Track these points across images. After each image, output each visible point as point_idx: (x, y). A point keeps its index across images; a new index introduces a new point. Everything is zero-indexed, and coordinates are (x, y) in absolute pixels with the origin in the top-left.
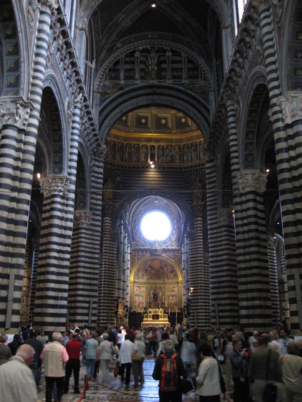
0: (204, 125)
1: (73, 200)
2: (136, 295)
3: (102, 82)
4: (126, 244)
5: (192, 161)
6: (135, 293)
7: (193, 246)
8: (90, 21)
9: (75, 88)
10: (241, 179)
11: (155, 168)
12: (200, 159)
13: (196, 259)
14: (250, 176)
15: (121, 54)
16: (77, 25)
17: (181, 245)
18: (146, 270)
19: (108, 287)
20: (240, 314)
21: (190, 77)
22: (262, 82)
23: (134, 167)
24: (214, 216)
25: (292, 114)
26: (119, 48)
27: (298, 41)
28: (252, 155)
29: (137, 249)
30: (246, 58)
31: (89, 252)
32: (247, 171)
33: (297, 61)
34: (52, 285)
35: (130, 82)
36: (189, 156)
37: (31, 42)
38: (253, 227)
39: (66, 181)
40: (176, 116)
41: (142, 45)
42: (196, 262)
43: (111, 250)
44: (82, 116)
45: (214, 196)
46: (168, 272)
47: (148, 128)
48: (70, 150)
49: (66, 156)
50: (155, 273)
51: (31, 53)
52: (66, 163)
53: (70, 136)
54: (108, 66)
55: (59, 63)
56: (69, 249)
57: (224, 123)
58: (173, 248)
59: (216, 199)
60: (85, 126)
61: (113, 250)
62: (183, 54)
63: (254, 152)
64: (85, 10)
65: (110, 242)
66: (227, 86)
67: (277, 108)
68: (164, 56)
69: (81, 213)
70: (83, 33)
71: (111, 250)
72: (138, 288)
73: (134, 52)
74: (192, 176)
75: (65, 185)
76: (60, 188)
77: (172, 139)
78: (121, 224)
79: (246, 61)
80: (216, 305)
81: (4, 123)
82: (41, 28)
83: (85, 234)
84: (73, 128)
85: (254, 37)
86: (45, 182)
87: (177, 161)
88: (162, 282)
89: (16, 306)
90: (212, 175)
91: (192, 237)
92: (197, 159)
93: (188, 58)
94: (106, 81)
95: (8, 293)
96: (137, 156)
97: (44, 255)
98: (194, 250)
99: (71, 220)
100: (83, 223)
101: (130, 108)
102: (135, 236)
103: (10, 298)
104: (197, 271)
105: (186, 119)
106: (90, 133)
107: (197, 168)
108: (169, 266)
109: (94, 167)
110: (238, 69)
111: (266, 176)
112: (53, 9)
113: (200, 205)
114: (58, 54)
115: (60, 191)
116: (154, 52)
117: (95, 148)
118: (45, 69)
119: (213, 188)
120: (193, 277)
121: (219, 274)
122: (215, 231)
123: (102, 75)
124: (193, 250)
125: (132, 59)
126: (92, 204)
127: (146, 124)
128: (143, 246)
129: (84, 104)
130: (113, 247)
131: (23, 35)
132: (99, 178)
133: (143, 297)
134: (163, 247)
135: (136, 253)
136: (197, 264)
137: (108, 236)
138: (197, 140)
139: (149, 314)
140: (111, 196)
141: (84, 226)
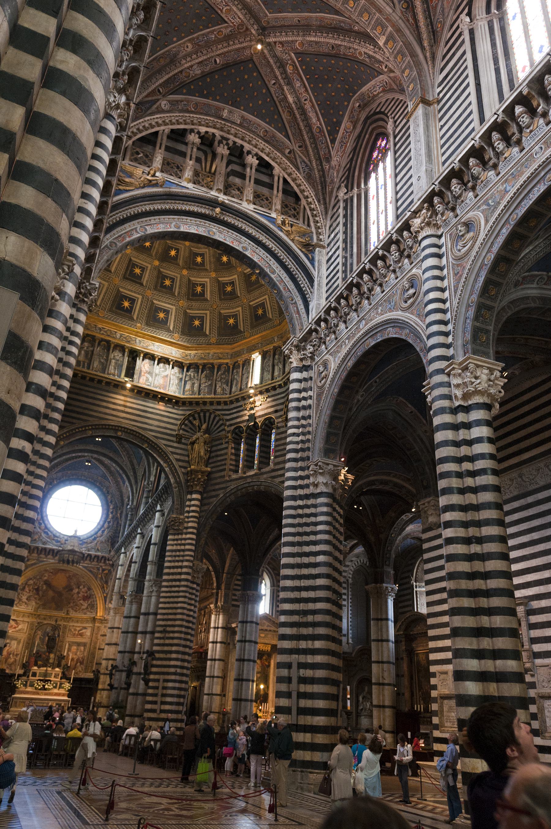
7: (176, 545)
12: (215, 394)
15: (165, 124)
18: (37, 590)
23: (92, 380)
26: (163, 111)
36: (196, 385)
40: (185, 313)
42: (178, 577)
46: (79, 597)
62: (277, 170)
88: (63, 615)
92: (209, 393)
96: (102, 361)
98: (178, 553)
107: (208, 407)
108: (84, 587)
116: (226, 147)
138: (216, 361)
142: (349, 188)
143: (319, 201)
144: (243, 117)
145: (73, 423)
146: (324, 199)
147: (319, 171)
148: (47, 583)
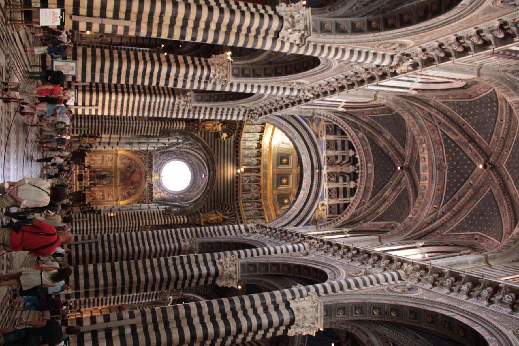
0: (283, 221)
1: (205, 88)
2: (103, 157)
3: (324, 118)
4: (157, 145)
5: (245, 211)
6: (105, 155)
7: (157, 215)
8: (384, 105)
9: (319, 90)
10: (231, 260)
11: (237, 173)
13: (144, 218)
14: (234, 270)
15: (352, 137)
16: (380, 93)
17: (157, 203)
18: (130, 167)
19: (112, 126)
20: (89, 265)
21: (330, 207)
22: (329, 277)
24: (190, 235)
25: (300, 307)
26: (357, 135)
27: (372, 309)
28: (256, 271)
29: (152, 157)
30: (352, 260)
31: (150, 106)
32: (239, 267)
33: (352, 310)
34: (116, 66)
35: (324, 146)
36: (249, 208)
37: (365, 45)
38: (181, 274)
39: (225, 81)
40: (290, 194)
41: (360, 157)
43: (151, 129)
44: (290, 97)
45: (211, 233)
47: (278, 165)
48: (256, 85)
49: (250, 81)
50: (126, 176)
51: (353, 46)
52: (243, 81)
53: (270, 85)
54: (339, 124)
55: (343, 73)
56: (154, 84)
57: (286, 242)
58: (154, 194)
59: (207, 236)
60: (279, 101)
61: (151, 131)
62: (352, 198)
63: (258, 273)
64: (395, 101)
65: (159, 128)
66: (324, 243)
67: (305, 292)
68: (351, 180)
69: (191, 96)
70: (372, 98)
71: (151, 129)
72: (111, 158)
73: (353, 149)
74: (230, 211)
75: (221, 80)
76: (217, 75)
77: (267, 190)
78: (178, 139)
79: (350, 261)
80: (96, 240)
81: (285, 18)
82: (378, 56)
83: (169, 102)
84: (278, 88)
85: (373, 267)
86: (224, 59)
87: (245, 196)
88: (118, 184)
89: (96, 27)
90: (232, 232)
91: (167, 213)
92: (246, 216)
93: (349, 203)
94: (325, 121)
95: (110, 18)
97: (148, 58)
99: (184, 86)
100: (180, 99)
101: (299, 146)
102: (165, 154)
103: (105, 21)
104: (131, 219)
105: (288, 204)
106: (273, 105)
107: (238, 217)
109: (238, 111)
110: (341, 252)
111: (234, 286)
112: (396, 68)
113: (200, 221)
114: (352, 73)
115: (215, 75)
116: (354, 170)
117: (258, 111)
118: (337, 60)
119: (219, 233)
120: (125, 216)
121: (129, 242)
122: (174, 236)
123: (330, 118)
124: (152, 214)
125: (347, 147)
126: (200, 108)
127: (282, 163)
128: (155, 163)
129: (302, 99)
130: (154, 131)
131: (372, 38)
132: (227, 115)
133: (101, 164)
134: (154, 184)
135: (148, 156)
136: (139, 220)
137: (166, 126)
139: (83, 171)
140: (207, 128)
141: (177, 100)
142: (349, 232)
143: (343, 223)
144: (371, 174)
145: (211, 147)
146: (344, 225)
147: (358, 219)
148: (134, 171)
